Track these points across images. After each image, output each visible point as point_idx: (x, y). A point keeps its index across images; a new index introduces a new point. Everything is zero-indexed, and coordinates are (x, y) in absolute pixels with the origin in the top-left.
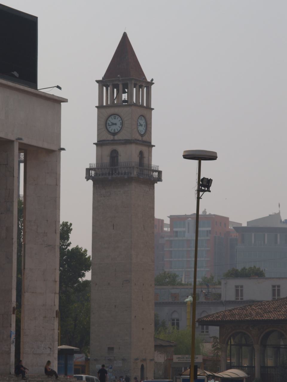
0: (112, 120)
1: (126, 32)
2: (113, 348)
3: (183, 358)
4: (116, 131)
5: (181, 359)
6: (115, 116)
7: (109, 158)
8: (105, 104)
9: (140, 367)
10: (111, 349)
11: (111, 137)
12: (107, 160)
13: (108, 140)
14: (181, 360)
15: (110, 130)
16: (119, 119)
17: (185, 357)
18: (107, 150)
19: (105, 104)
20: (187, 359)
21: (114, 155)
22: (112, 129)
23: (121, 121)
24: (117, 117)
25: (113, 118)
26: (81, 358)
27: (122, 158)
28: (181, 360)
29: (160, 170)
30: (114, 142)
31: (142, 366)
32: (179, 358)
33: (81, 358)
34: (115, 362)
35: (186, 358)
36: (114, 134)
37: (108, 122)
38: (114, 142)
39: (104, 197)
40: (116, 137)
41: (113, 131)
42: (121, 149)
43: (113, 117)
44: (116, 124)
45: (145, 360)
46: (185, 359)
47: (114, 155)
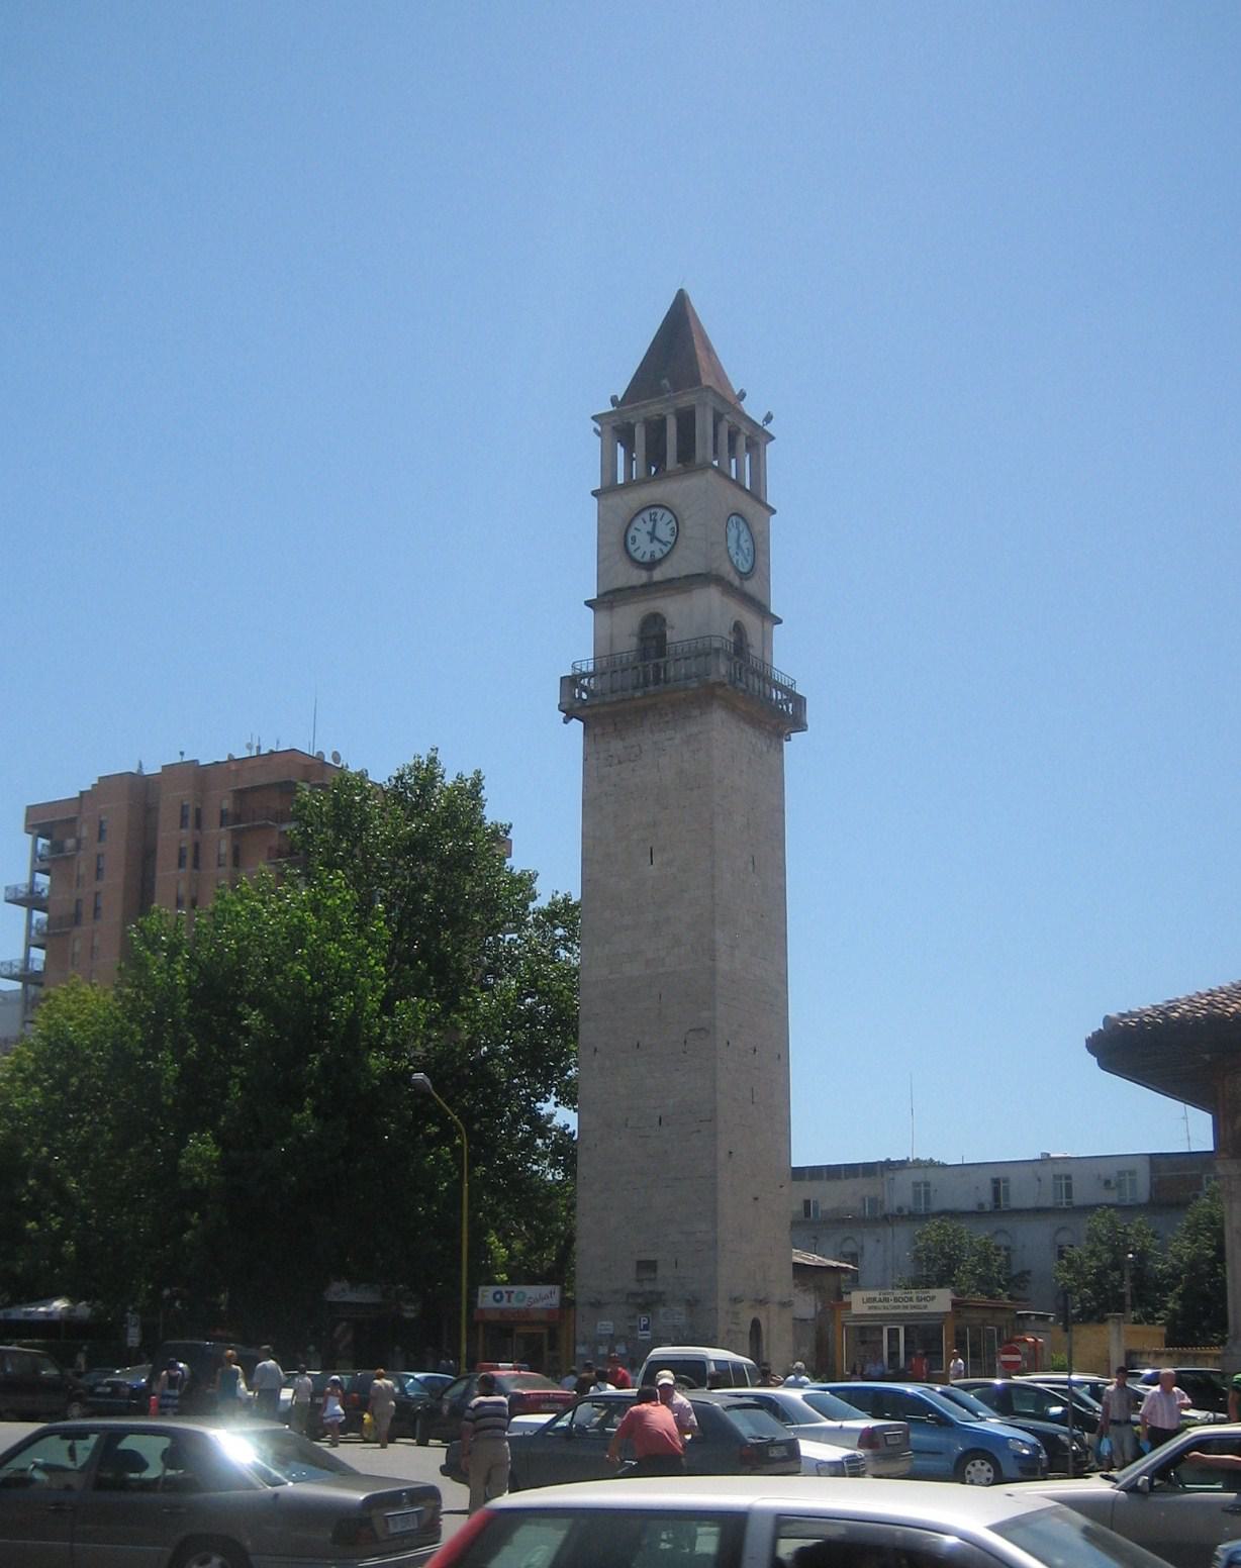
1: (684, 287)
2: (655, 1261)
3: (887, 1300)
4: (658, 555)
7: (635, 640)
8: (620, 480)
9: (747, 1328)
10: (647, 1266)
11: (639, 577)
12: (628, 644)
14: (875, 1308)
15: (638, 555)
16: (668, 516)
18: (629, 617)
19: (620, 480)
20: (896, 1304)
21: (653, 632)
22: (644, 548)
23: (674, 524)
24: (660, 512)
26: (546, 1297)
28: (875, 1308)
30: (649, 588)
31: (756, 1324)
32: (870, 1300)
33: (546, 1297)
34: (662, 1310)
35: (896, 1300)
36: (651, 565)
37: (632, 532)
38: (649, 588)
40: (658, 575)
41: (647, 558)
42: (672, 607)
43: (646, 515)
46: (892, 1303)
47: (653, 632)
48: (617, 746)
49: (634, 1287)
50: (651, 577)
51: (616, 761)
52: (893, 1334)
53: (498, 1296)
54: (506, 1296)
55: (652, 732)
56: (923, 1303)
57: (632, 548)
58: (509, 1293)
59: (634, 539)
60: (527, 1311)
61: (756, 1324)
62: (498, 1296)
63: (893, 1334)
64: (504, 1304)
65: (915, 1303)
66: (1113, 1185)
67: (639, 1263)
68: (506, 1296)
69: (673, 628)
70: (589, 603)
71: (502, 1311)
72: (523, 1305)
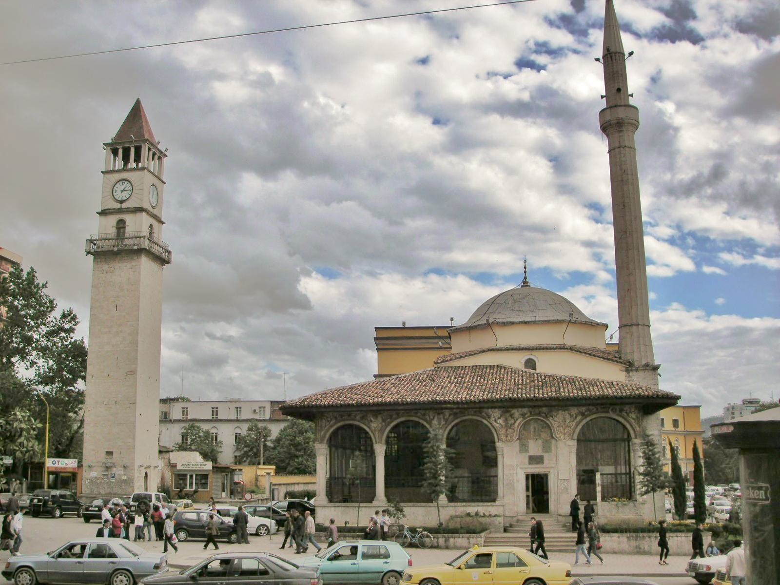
0: (120, 187)
4: (125, 199)
6: (123, 182)
9: (144, 475)
10: (110, 453)
11: (118, 206)
13: (114, 209)
14: (186, 467)
15: (117, 197)
22: (119, 196)
24: (126, 182)
25: (121, 184)
27: (130, 230)
28: (186, 467)
29: (170, 249)
30: (120, 211)
31: (146, 474)
36: (122, 202)
38: (120, 211)
39: (106, 273)
40: (124, 206)
41: (120, 199)
42: (128, 218)
43: (121, 183)
44: (122, 191)
45: (149, 467)
48: (105, 267)
49: (104, 461)
50: (121, 206)
51: (105, 272)
52: (191, 476)
53: (54, 462)
54: (57, 462)
55: (119, 263)
56: (202, 466)
57: (115, 194)
58: (58, 461)
59: (116, 191)
60: (65, 468)
61: (146, 474)
62: (54, 462)
63: (191, 476)
64: (56, 465)
65: (199, 466)
66: (257, 412)
67: (107, 452)
68: (57, 462)
69: (128, 226)
70: (98, 213)
71: (56, 468)
72: (64, 466)
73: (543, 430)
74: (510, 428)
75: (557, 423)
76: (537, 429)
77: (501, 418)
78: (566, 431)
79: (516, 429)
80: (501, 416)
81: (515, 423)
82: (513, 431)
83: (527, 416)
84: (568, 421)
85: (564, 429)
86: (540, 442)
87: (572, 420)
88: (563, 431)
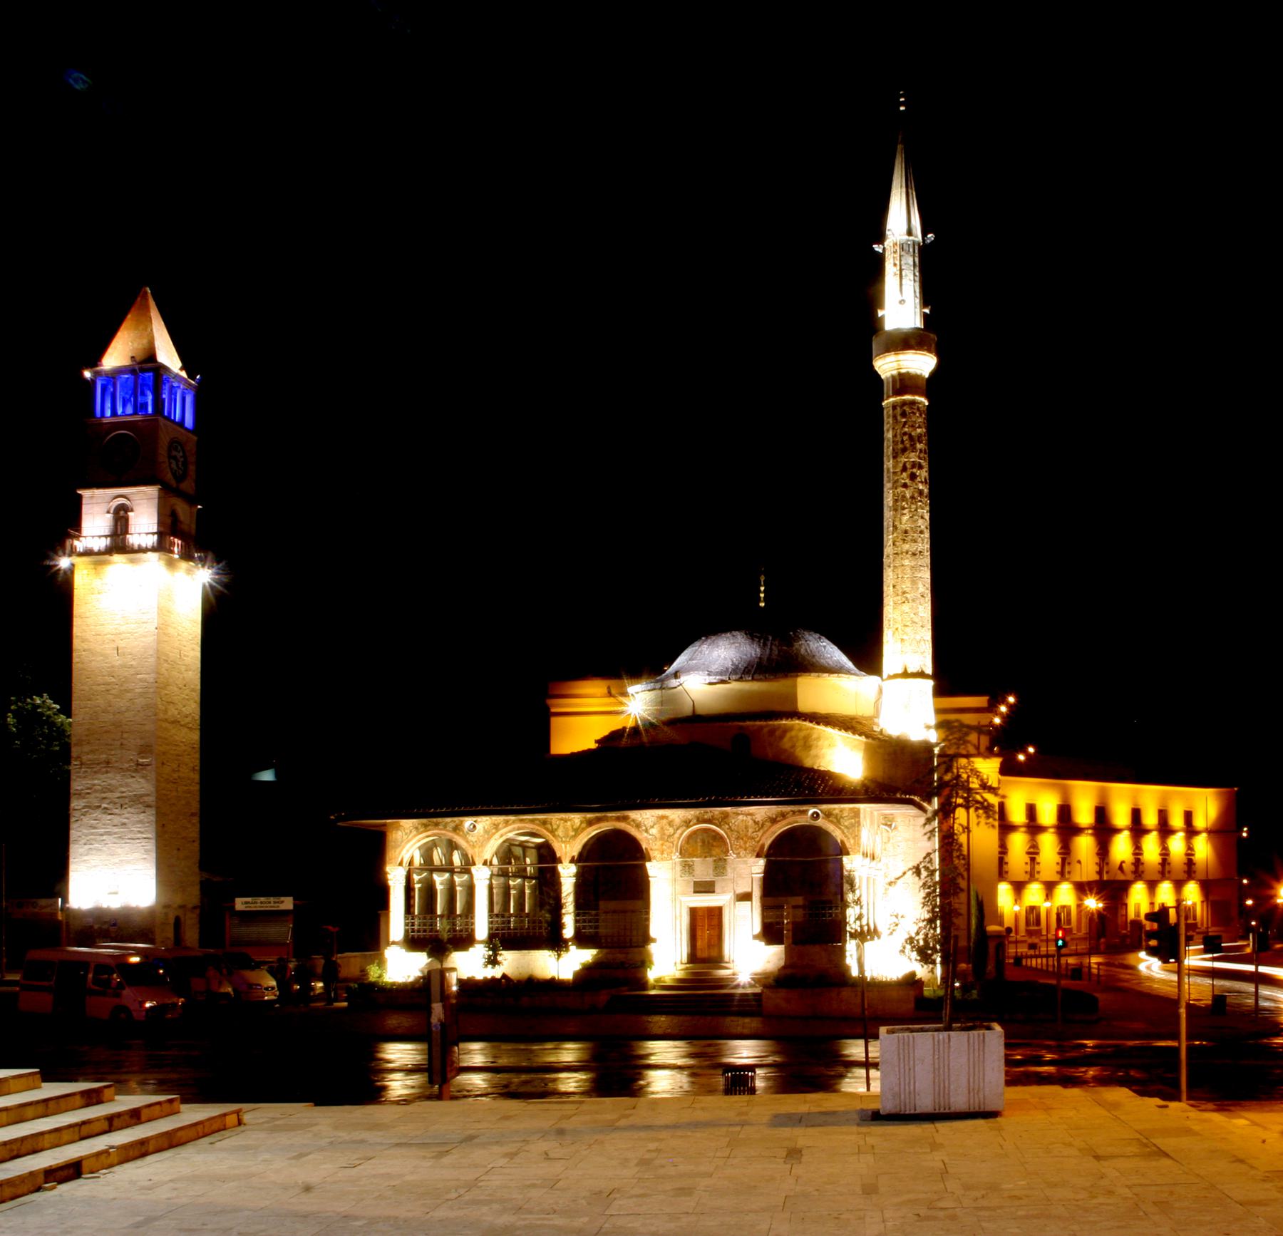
5: (252, 905)
14: (250, 907)
17: (259, 901)
28: (250, 907)
32: (246, 903)
35: (261, 903)
46: (259, 905)
56: (277, 905)
65: (272, 905)
73: (715, 844)
74: (668, 841)
75: (736, 833)
76: (706, 843)
77: (655, 826)
78: (747, 846)
79: (675, 843)
80: (654, 824)
81: (674, 834)
82: (671, 845)
83: (691, 823)
84: (750, 830)
85: (745, 843)
86: (710, 860)
87: (757, 829)
88: (743, 846)
